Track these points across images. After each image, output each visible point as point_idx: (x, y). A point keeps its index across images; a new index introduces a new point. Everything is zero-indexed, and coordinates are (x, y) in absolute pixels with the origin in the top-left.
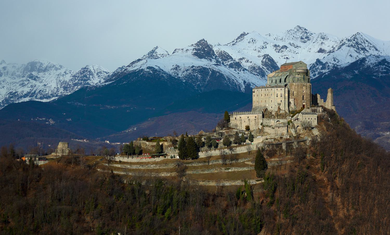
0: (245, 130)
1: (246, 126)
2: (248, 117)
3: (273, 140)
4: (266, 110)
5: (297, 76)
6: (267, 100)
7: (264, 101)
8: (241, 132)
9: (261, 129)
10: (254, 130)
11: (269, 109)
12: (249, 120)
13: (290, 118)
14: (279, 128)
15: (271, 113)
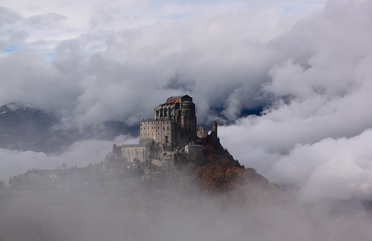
0: (133, 162)
1: (134, 159)
2: (136, 150)
3: (160, 172)
4: (154, 142)
5: (183, 109)
6: (154, 132)
7: (151, 134)
8: (130, 164)
9: (148, 161)
10: (142, 162)
11: (157, 141)
12: (137, 152)
13: (177, 150)
14: (166, 160)
15: (158, 145)
